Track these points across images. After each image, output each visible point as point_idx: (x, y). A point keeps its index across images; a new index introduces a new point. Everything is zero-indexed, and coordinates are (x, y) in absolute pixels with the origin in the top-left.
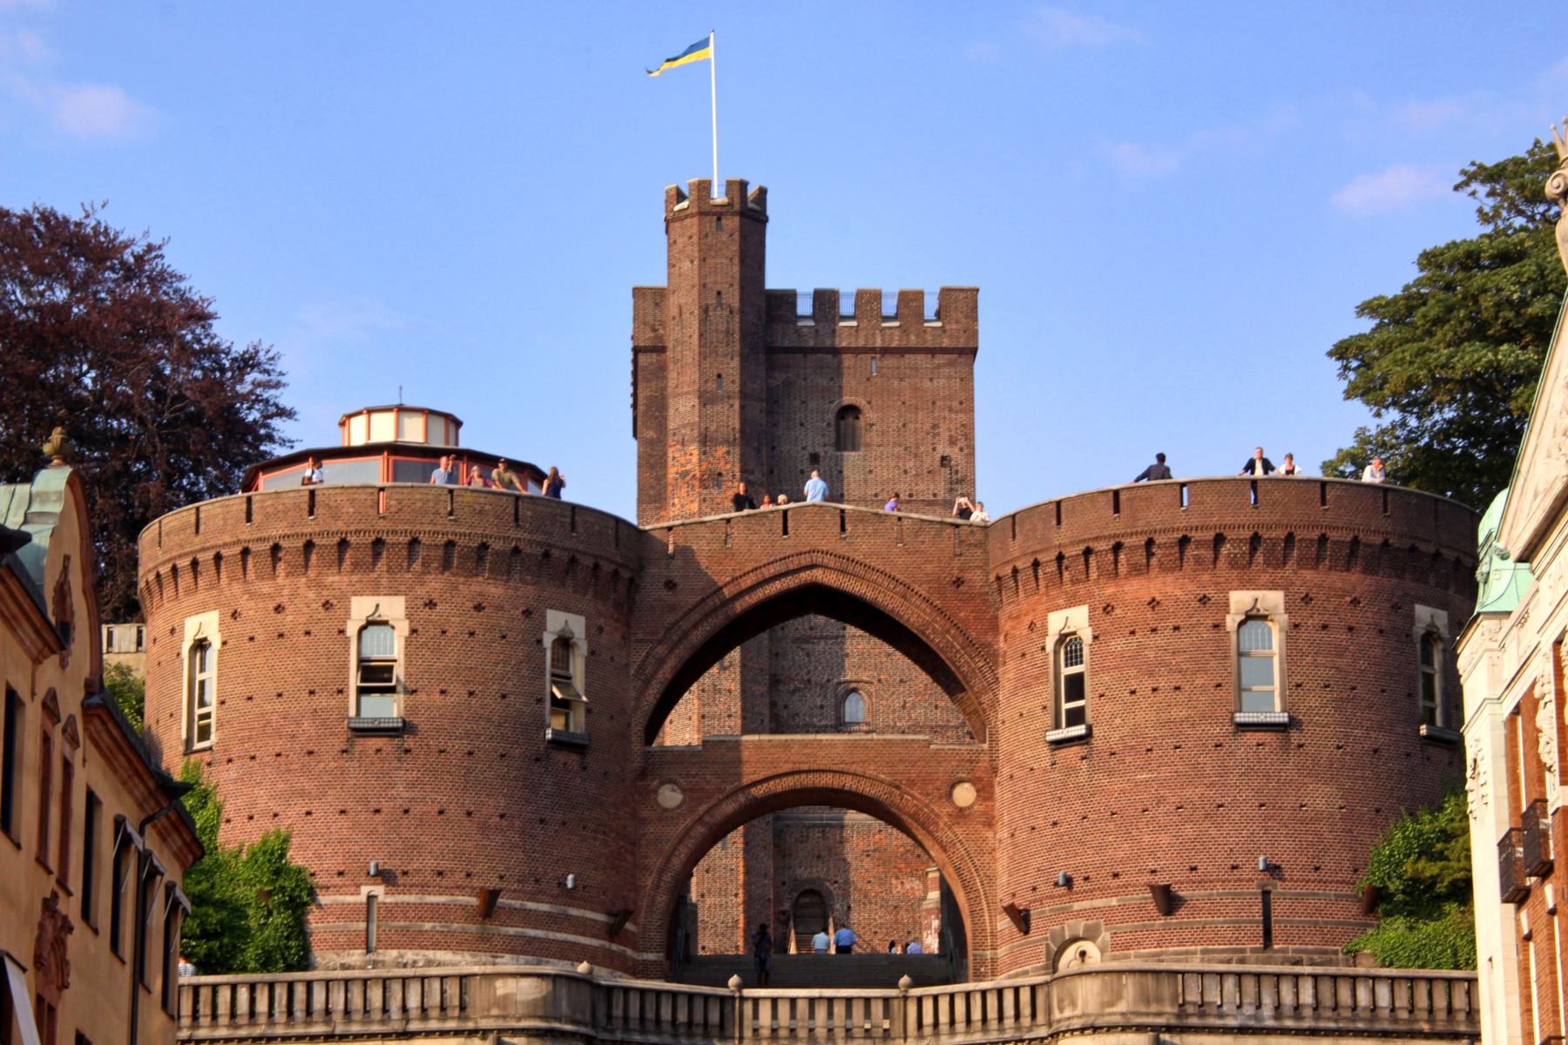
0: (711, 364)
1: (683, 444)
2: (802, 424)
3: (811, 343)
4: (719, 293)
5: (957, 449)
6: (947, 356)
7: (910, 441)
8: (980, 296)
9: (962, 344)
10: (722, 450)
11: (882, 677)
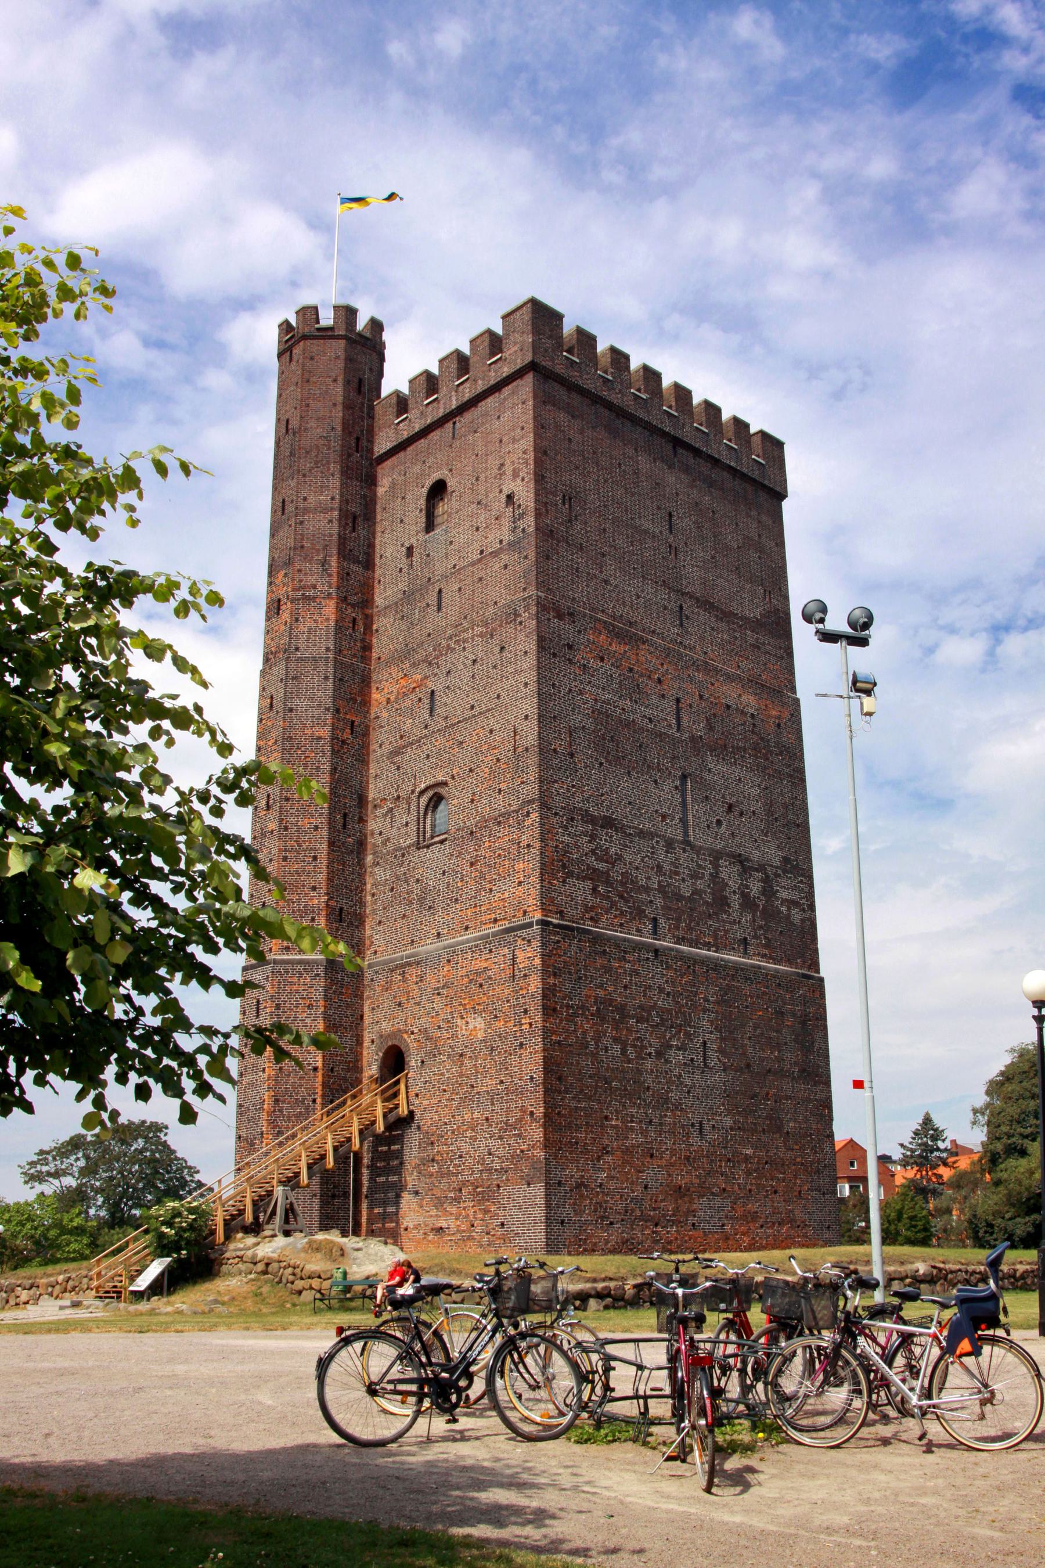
4: (288, 421)
5: (519, 480)
6: (510, 387)
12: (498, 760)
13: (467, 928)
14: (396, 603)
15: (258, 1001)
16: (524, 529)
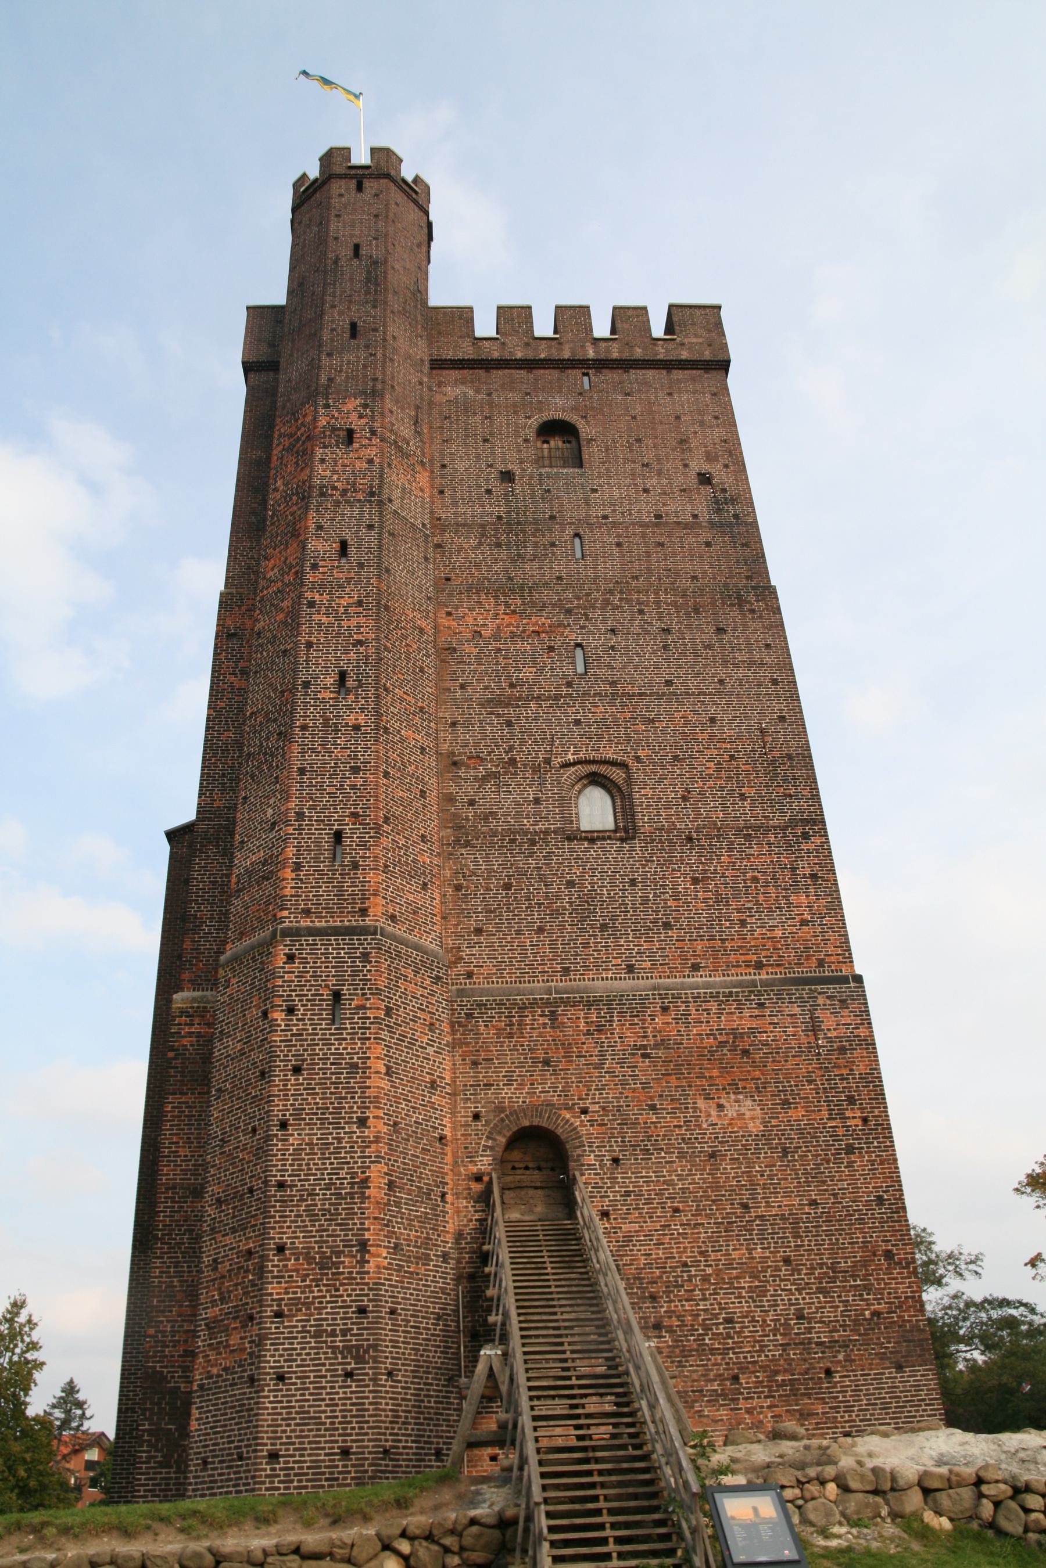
0: (341, 313)
1: (293, 414)
2: (486, 441)
3: (496, 355)
4: (357, 248)
7: (649, 456)
8: (723, 313)
9: (707, 355)
10: (352, 404)
11: (640, 753)
12: (732, 757)
13: (696, 967)
14: (483, 526)
15: (337, 996)
16: (736, 516)
